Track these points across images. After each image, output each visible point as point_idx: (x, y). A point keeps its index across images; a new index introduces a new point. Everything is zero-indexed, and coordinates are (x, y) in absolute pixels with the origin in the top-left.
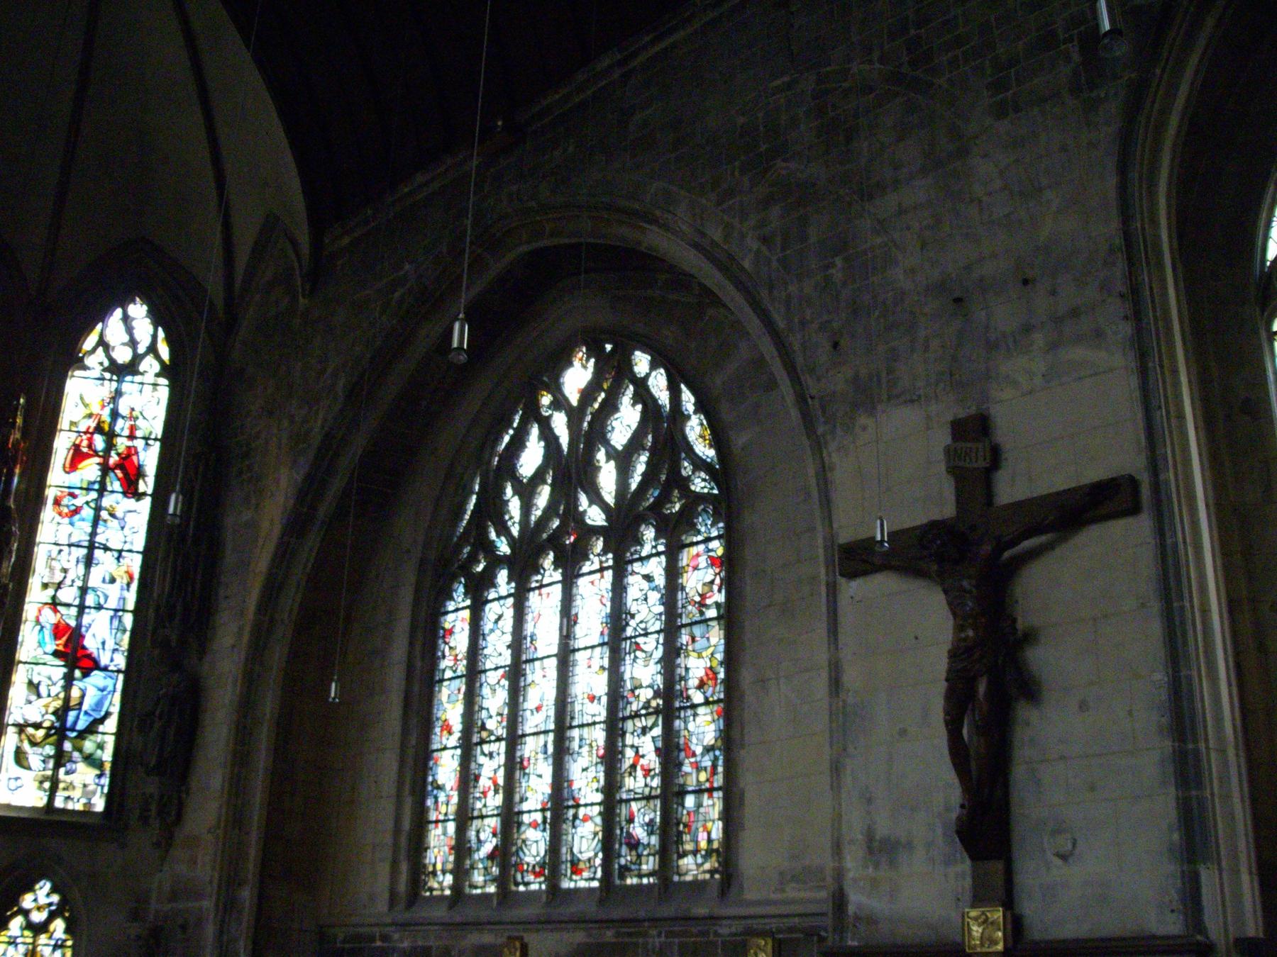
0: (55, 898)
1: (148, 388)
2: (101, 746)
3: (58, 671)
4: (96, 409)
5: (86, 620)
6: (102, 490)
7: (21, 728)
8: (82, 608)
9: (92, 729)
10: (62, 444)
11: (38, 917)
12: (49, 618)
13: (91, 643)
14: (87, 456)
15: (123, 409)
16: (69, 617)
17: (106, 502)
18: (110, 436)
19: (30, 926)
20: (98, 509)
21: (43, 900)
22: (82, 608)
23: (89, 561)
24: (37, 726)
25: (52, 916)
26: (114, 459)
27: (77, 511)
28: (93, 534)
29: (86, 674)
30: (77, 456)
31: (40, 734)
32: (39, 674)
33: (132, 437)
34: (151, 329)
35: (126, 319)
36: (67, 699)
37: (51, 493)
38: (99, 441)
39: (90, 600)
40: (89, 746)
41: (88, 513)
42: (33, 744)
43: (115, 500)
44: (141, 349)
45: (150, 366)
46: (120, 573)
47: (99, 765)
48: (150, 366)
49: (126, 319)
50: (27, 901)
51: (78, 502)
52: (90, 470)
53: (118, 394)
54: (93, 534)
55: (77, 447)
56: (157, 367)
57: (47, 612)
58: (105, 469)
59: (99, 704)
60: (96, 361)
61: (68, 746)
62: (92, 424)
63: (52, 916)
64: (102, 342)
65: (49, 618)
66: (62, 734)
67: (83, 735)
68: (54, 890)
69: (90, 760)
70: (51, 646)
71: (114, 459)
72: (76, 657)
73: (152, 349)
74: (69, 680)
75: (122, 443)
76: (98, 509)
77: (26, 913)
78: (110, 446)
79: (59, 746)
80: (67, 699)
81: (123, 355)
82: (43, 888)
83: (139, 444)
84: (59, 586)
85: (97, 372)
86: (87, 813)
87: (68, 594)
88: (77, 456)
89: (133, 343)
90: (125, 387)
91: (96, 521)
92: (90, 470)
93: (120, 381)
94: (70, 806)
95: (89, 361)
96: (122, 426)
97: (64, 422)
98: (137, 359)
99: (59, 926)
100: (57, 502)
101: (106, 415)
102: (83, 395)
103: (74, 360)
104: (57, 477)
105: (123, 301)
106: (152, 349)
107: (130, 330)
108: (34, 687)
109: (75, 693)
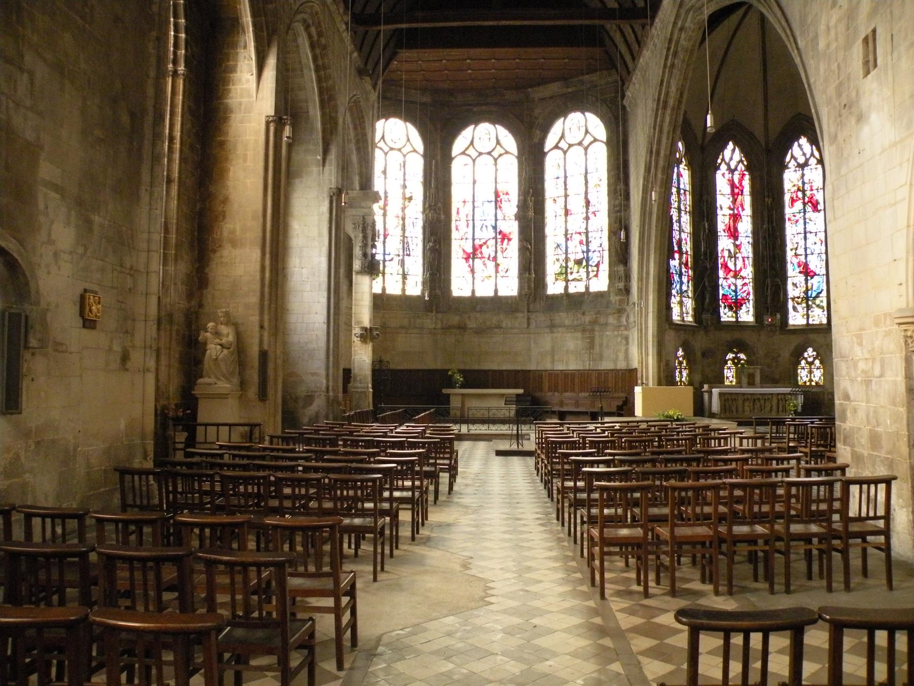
0: (815, 353)
1: (814, 170)
2: (822, 301)
3: (802, 278)
4: (796, 183)
5: (809, 258)
6: (805, 212)
7: (793, 299)
8: (806, 255)
9: (817, 296)
10: (787, 198)
11: (810, 360)
12: (795, 261)
13: (812, 267)
14: (796, 201)
15: (806, 180)
16: (802, 259)
17: (807, 216)
18: (804, 191)
19: (807, 363)
20: (805, 219)
21: (811, 354)
22: (806, 255)
23: (805, 238)
24: (798, 298)
25: (815, 359)
26: (807, 200)
27: (797, 221)
28: (805, 228)
29: (812, 277)
30: (793, 201)
31: (800, 300)
32: (796, 280)
33: (812, 190)
34: (810, 147)
35: (800, 146)
36: (807, 287)
37: (787, 217)
38: (800, 194)
39: (809, 252)
40: (818, 301)
41: (801, 221)
42: (798, 304)
43: (810, 214)
44: (808, 156)
45: (813, 161)
46: (817, 240)
47: (823, 308)
48: (813, 161)
49: (800, 146)
50: (806, 355)
51: (797, 218)
52: (799, 205)
53: (803, 175)
54: (805, 228)
55: (792, 198)
56: (815, 161)
57: (794, 258)
58: (804, 204)
59: (819, 287)
60: (792, 164)
61: (810, 303)
62: (796, 188)
63: (815, 359)
64: (792, 157)
65: (795, 261)
66: (807, 299)
67: (815, 298)
68: (814, 351)
69: (818, 306)
70: (798, 270)
71: (807, 200)
72: (807, 272)
73: (812, 155)
74: (806, 280)
75: (808, 193)
76: (805, 219)
77: (806, 359)
78: (804, 195)
79: (807, 303)
80: (807, 287)
81: (801, 160)
82: (810, 350)
83: (815, 192)
84: (796, 249)
85: (793, 168)
86: (821, 324)
87: (801, 251)
88: (793, 201)
89: (804, 154)
90: (805, 172)
91: (805, 223)
92: (799, 205)
93: (803, 170)
94: (815, 323)
95: (790, 165)
96: (807, 187)
97: (786, 191)
98: (807, 160)
99: (817, 362)
100: (789, 219)
101: (800, 185)
102: (790, 178)
103: (783, 167)
104: (788, 211)
105: (797, 139)
106: (812, 155)
107: (802, 149)
108: (795, 285)
109: (809, 285)
